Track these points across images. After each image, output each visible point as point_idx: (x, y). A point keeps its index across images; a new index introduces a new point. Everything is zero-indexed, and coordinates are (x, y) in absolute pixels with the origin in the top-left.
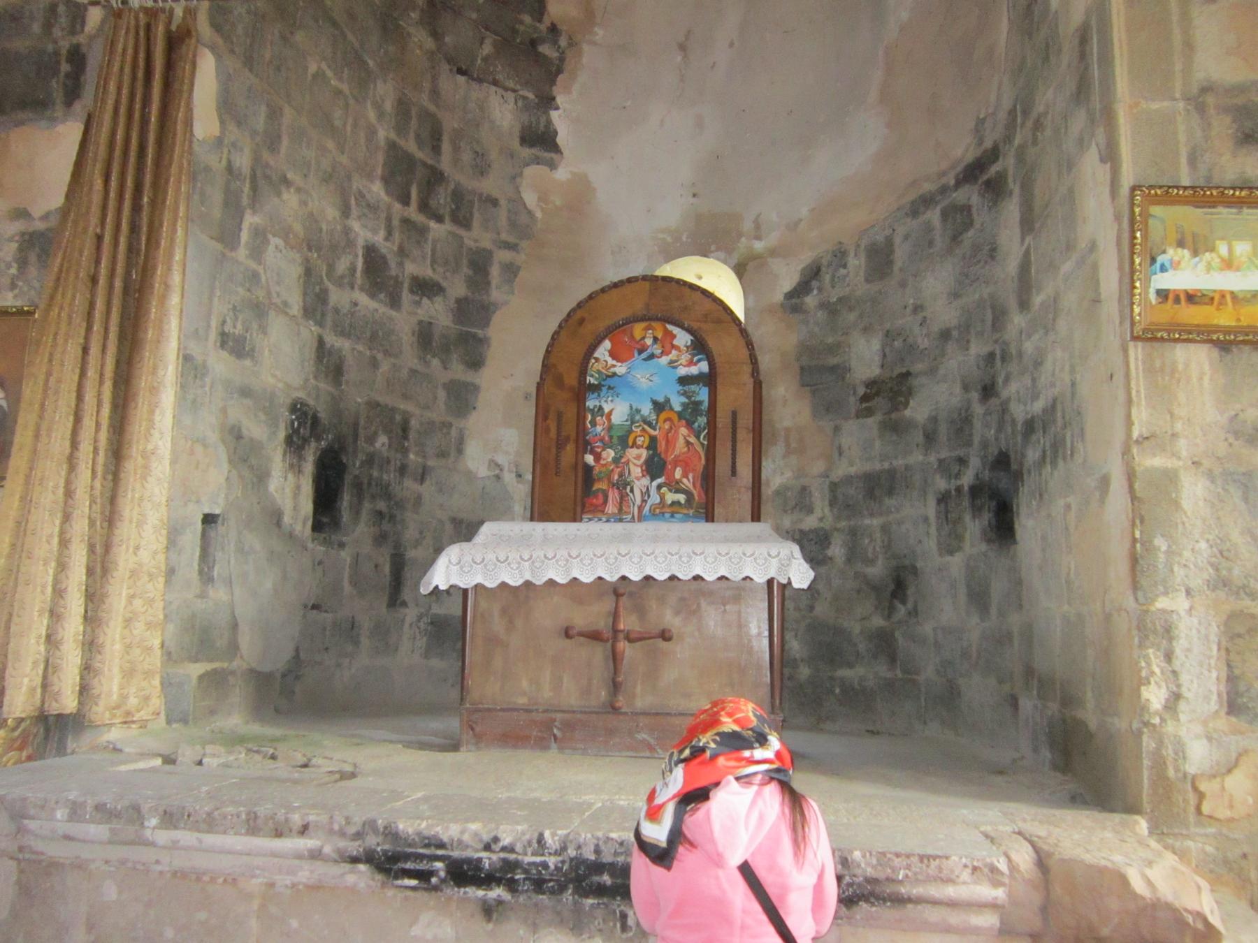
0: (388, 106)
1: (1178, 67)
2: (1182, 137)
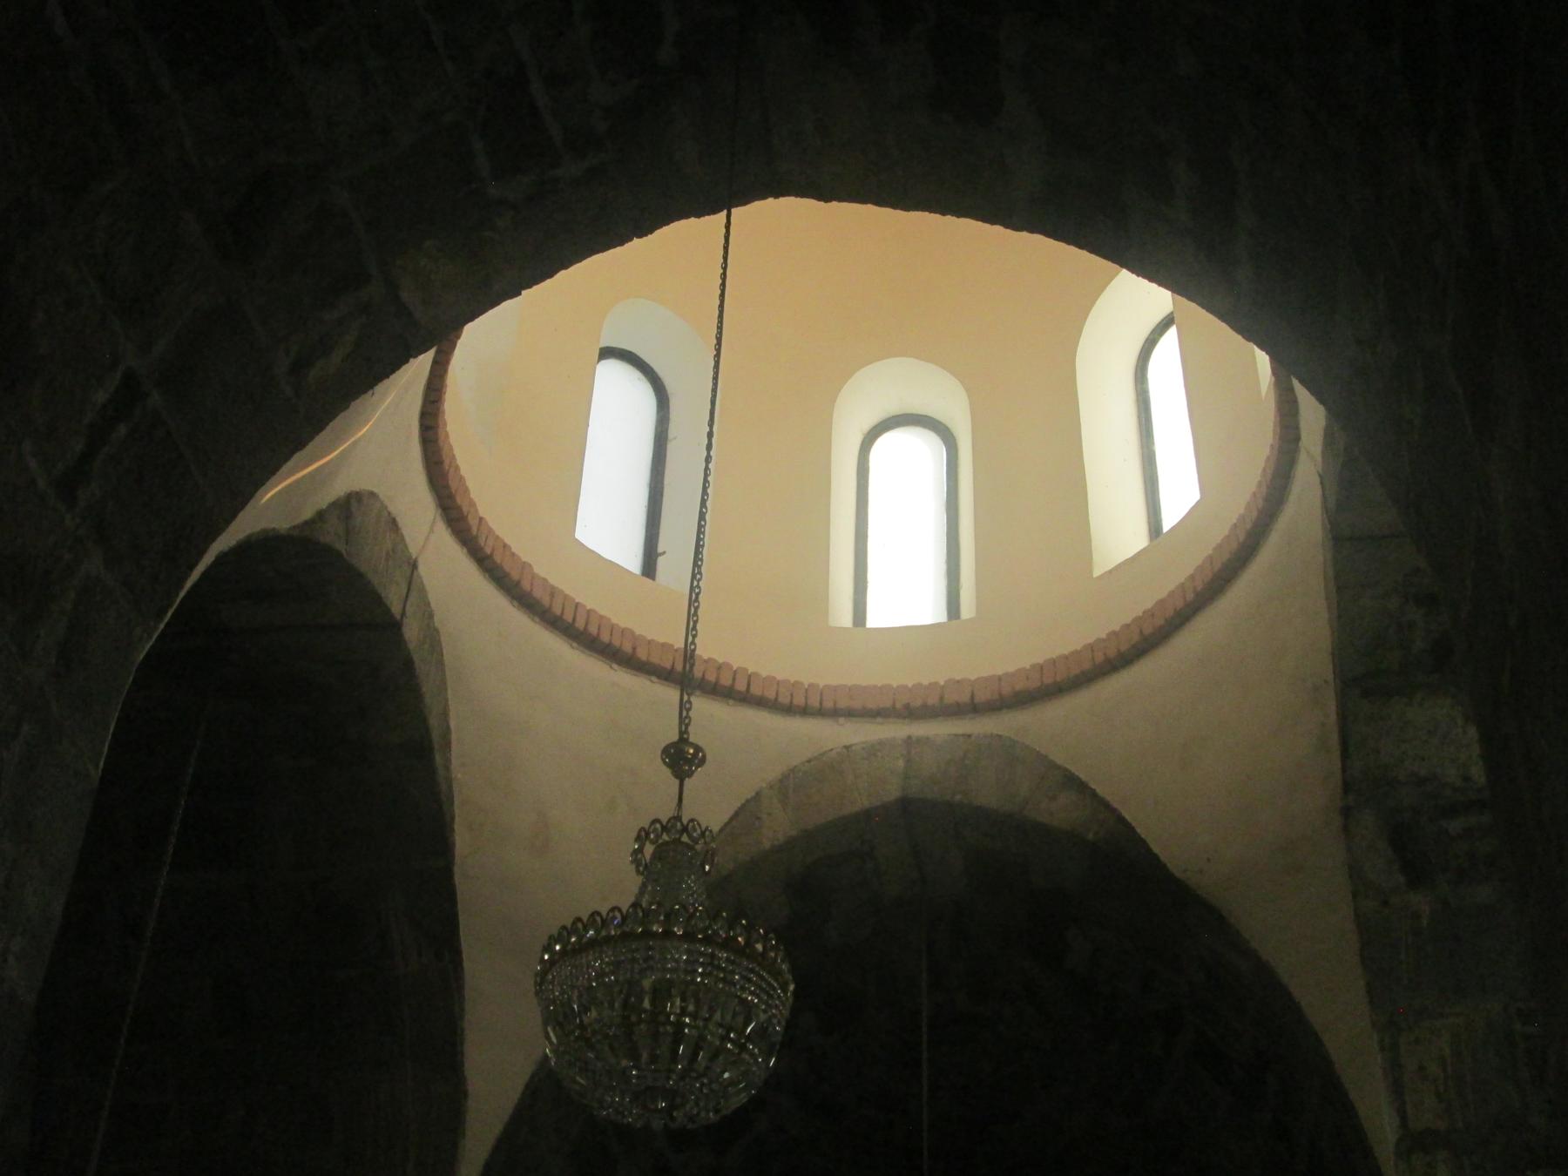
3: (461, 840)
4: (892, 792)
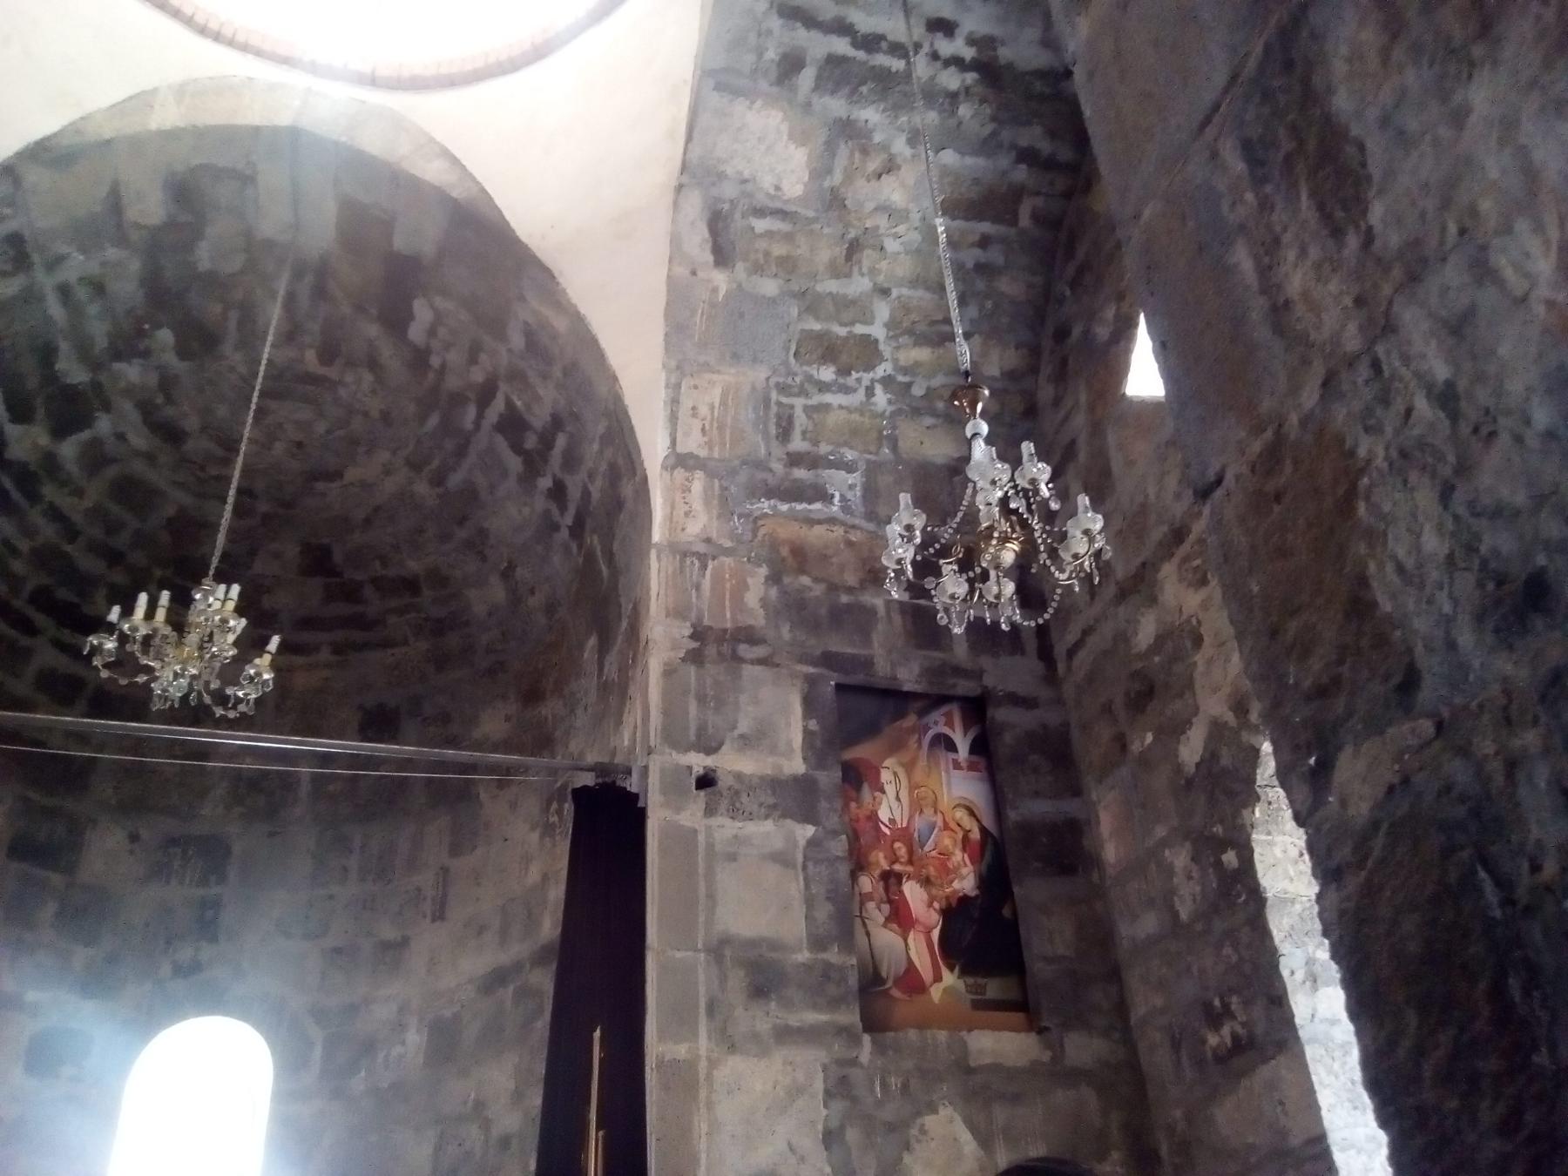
1: (702, 919)
2: (702, 990)
4: (284, 119)
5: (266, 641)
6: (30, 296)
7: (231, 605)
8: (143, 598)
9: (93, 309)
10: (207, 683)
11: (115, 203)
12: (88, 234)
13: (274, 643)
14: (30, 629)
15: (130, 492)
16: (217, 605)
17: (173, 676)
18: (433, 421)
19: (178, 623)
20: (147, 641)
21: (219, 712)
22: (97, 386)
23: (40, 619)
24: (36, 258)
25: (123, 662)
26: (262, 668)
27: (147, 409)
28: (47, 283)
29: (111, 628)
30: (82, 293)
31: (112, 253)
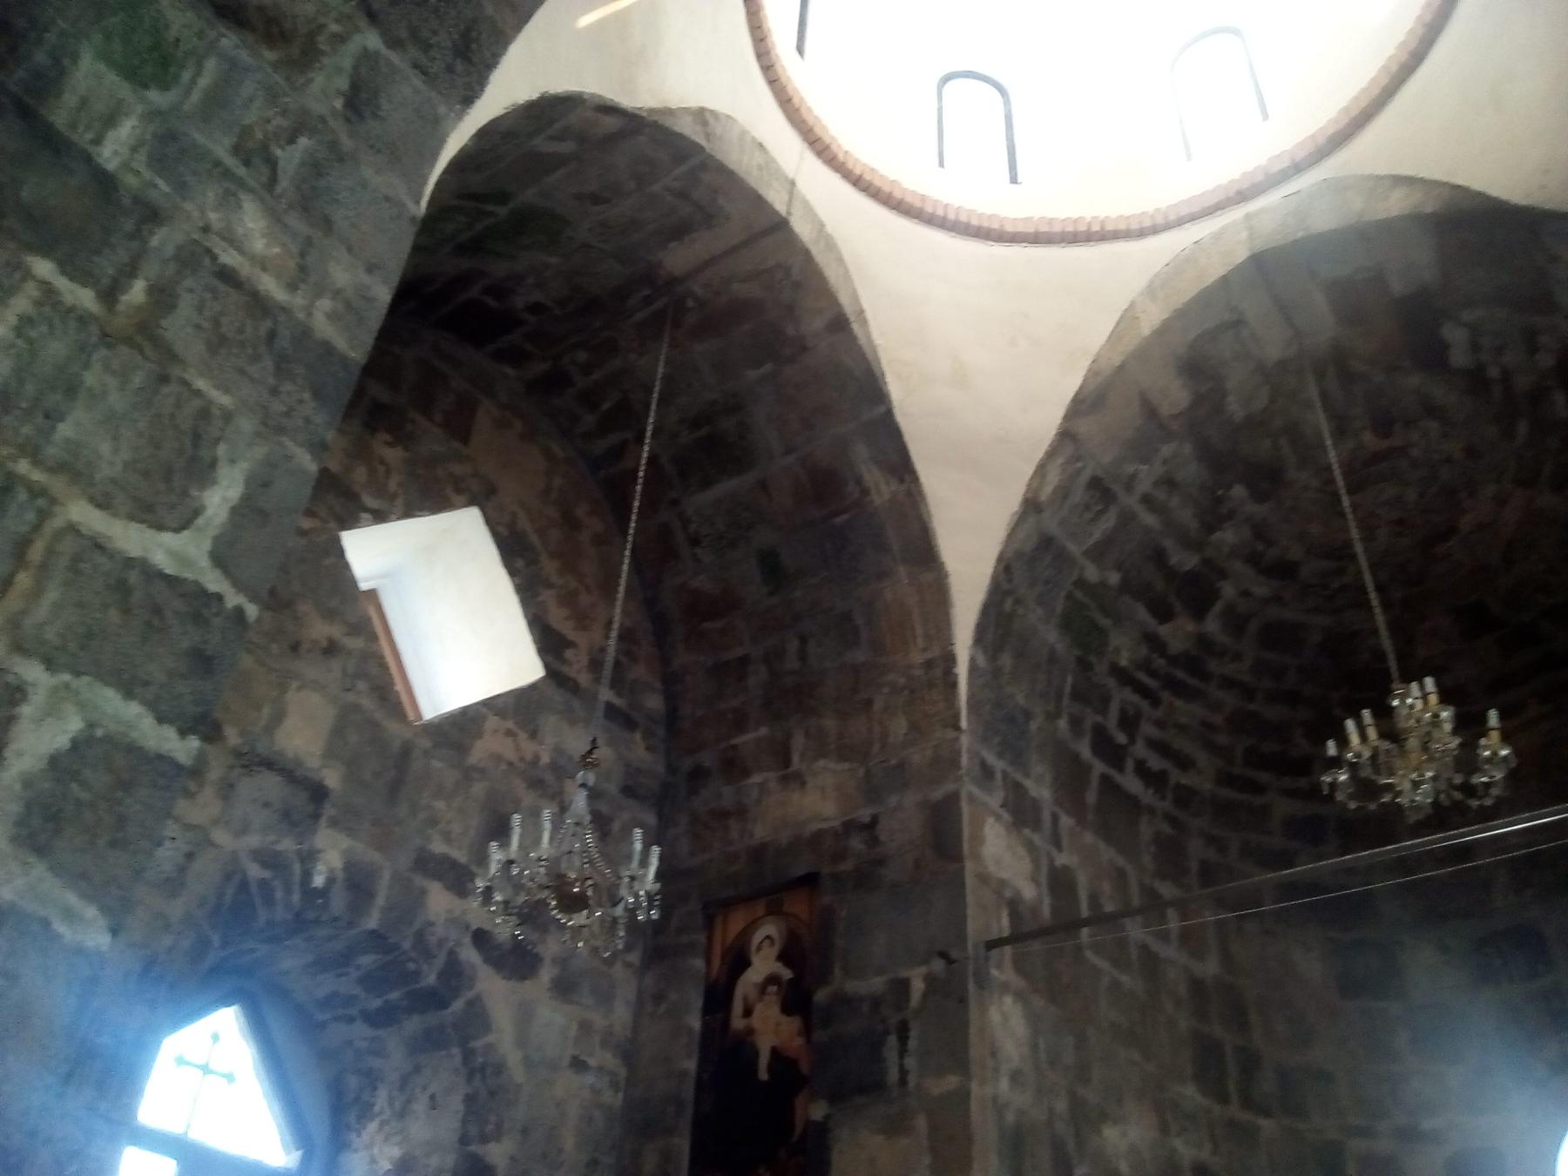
0: (1182, 990)
3: (896, 390)
4: (1241, 255)
5: (1483, 719)
6: (1127, 518)
7: (1433, 699)
8: (1350, 724)
9: (1175, 502)
10: (1449, 780)
11: (1150, 411)
12: (1141, 448)
13: (1493, 717)
14: (1258, 789)
15: (1277, 636)
16: (1419, 705)
17: (1415, 785)
18: (1522, 428)
19: (1391, 733)
20: (1374, 757)
21: (1474, 803)
22: (1206, 562)
23: (1264, 777)
24: (1117, 488)
25: (1366, 788)
26: (1494, 747)
27: (1253, 559)
28: (1131, 501)
29: (1336, 763)
30: (1161, 495)
31: (1166, 450)
